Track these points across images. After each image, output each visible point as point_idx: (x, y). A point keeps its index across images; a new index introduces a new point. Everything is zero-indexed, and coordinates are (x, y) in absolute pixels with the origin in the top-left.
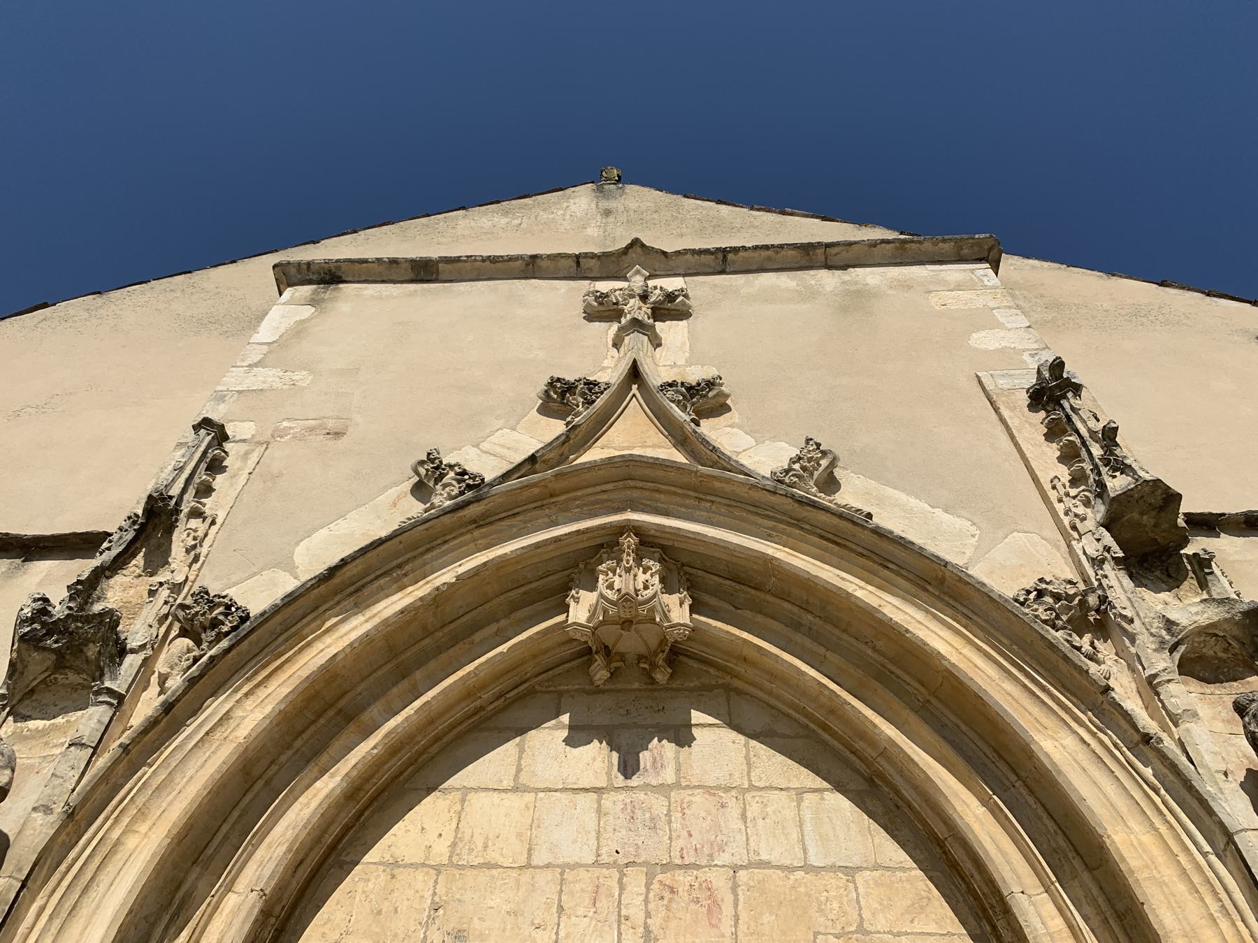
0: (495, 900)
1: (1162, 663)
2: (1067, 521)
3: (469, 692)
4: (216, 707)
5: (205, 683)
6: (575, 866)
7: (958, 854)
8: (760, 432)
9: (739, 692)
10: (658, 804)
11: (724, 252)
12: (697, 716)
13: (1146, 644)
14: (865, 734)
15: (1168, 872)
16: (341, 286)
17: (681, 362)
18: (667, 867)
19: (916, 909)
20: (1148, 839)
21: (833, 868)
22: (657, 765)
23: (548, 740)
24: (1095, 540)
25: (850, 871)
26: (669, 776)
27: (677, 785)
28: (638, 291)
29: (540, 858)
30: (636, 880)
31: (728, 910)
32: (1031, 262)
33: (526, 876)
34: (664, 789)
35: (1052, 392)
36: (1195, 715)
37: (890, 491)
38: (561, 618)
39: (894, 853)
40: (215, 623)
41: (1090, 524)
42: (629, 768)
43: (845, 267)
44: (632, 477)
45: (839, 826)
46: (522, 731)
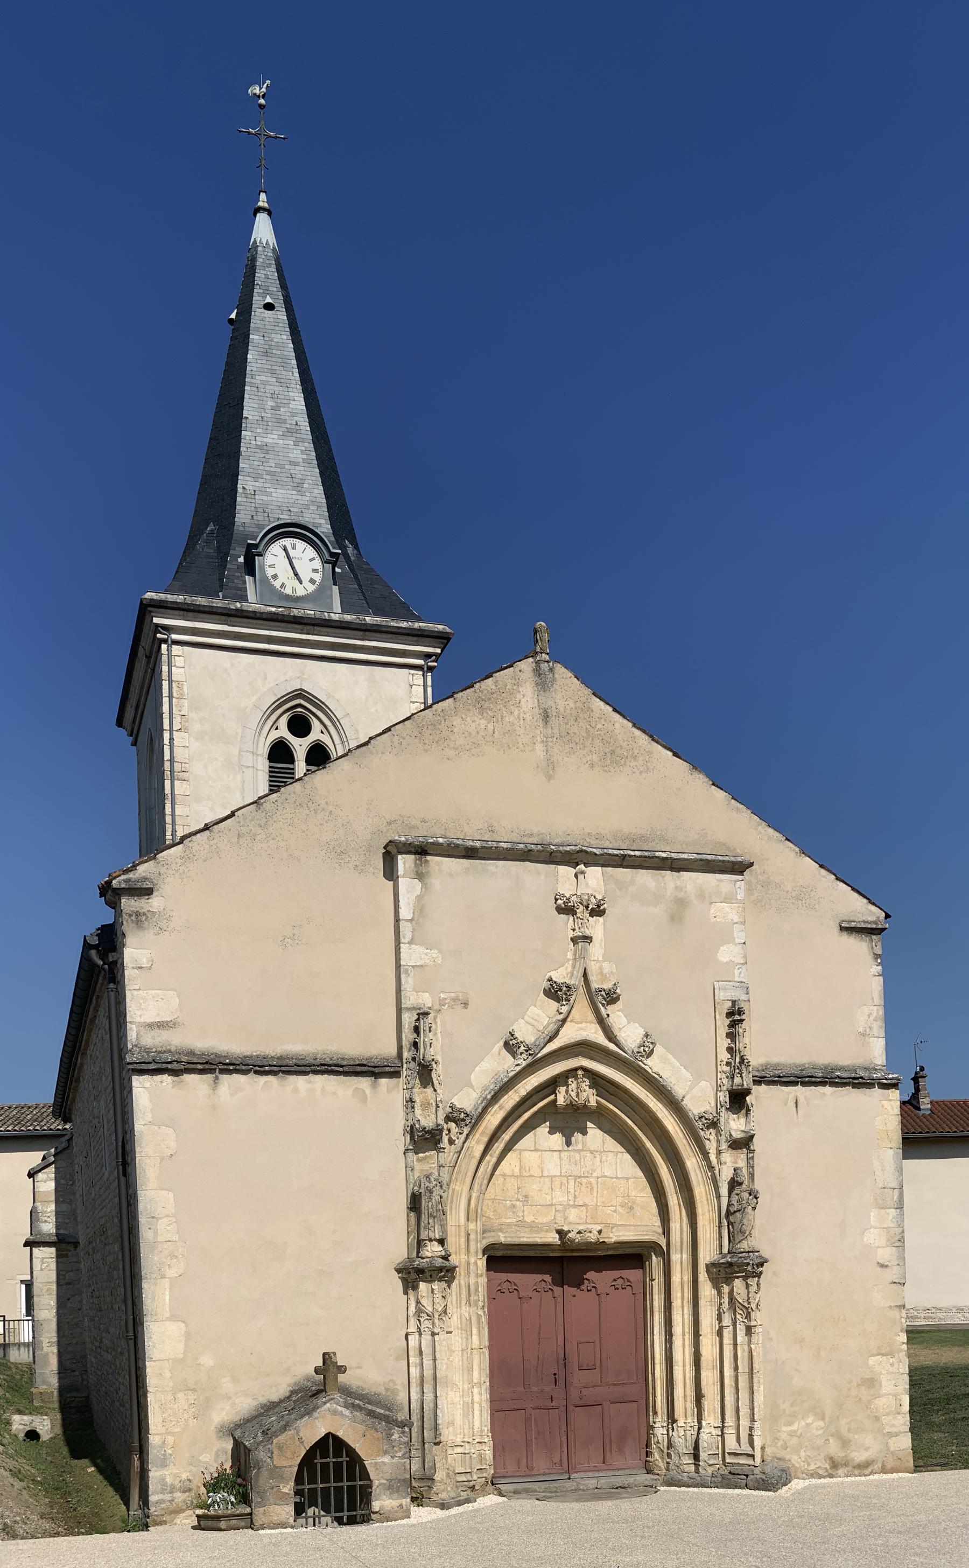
0: (535, 1187)
1: (724, 1146)
2: (719, 1082)
6: (555, 1176)
7: (657, 1179)
9: (603, 1115)
10: (577, 1156)
11: (624, 856)
12: (589, 1124)
13: (723, 1139)
14: (644, 1146)
15: (705, 1198)
16: (429, 858)
17: (600, 959)
18: (580, 1177)
19: (642, 1190)
20: (703, 1190)
21: (623, 1178)
22: (577, 1142)
23: (543, 1130)
24: (724, 1097)
25: (627, 1179)
26: (580, 1146)
27: (582, 1150)
28: (585, 903)
29: (546, 1174)
30: (572, 1182)
31: (595, 1190)
32: (771, 831)
33: (542, 1180)
34: (579, 1151)
35: (735, 1016)
36: (725, 1163)
37: (670, 1056)
38: (553, 1097)
39: (640, 1174)
40: (463, 1120)
41: (724, 1088)
42: (568, 1143)
44: (583, 1047)
45: (626, 1164)
46: (534, 1128)
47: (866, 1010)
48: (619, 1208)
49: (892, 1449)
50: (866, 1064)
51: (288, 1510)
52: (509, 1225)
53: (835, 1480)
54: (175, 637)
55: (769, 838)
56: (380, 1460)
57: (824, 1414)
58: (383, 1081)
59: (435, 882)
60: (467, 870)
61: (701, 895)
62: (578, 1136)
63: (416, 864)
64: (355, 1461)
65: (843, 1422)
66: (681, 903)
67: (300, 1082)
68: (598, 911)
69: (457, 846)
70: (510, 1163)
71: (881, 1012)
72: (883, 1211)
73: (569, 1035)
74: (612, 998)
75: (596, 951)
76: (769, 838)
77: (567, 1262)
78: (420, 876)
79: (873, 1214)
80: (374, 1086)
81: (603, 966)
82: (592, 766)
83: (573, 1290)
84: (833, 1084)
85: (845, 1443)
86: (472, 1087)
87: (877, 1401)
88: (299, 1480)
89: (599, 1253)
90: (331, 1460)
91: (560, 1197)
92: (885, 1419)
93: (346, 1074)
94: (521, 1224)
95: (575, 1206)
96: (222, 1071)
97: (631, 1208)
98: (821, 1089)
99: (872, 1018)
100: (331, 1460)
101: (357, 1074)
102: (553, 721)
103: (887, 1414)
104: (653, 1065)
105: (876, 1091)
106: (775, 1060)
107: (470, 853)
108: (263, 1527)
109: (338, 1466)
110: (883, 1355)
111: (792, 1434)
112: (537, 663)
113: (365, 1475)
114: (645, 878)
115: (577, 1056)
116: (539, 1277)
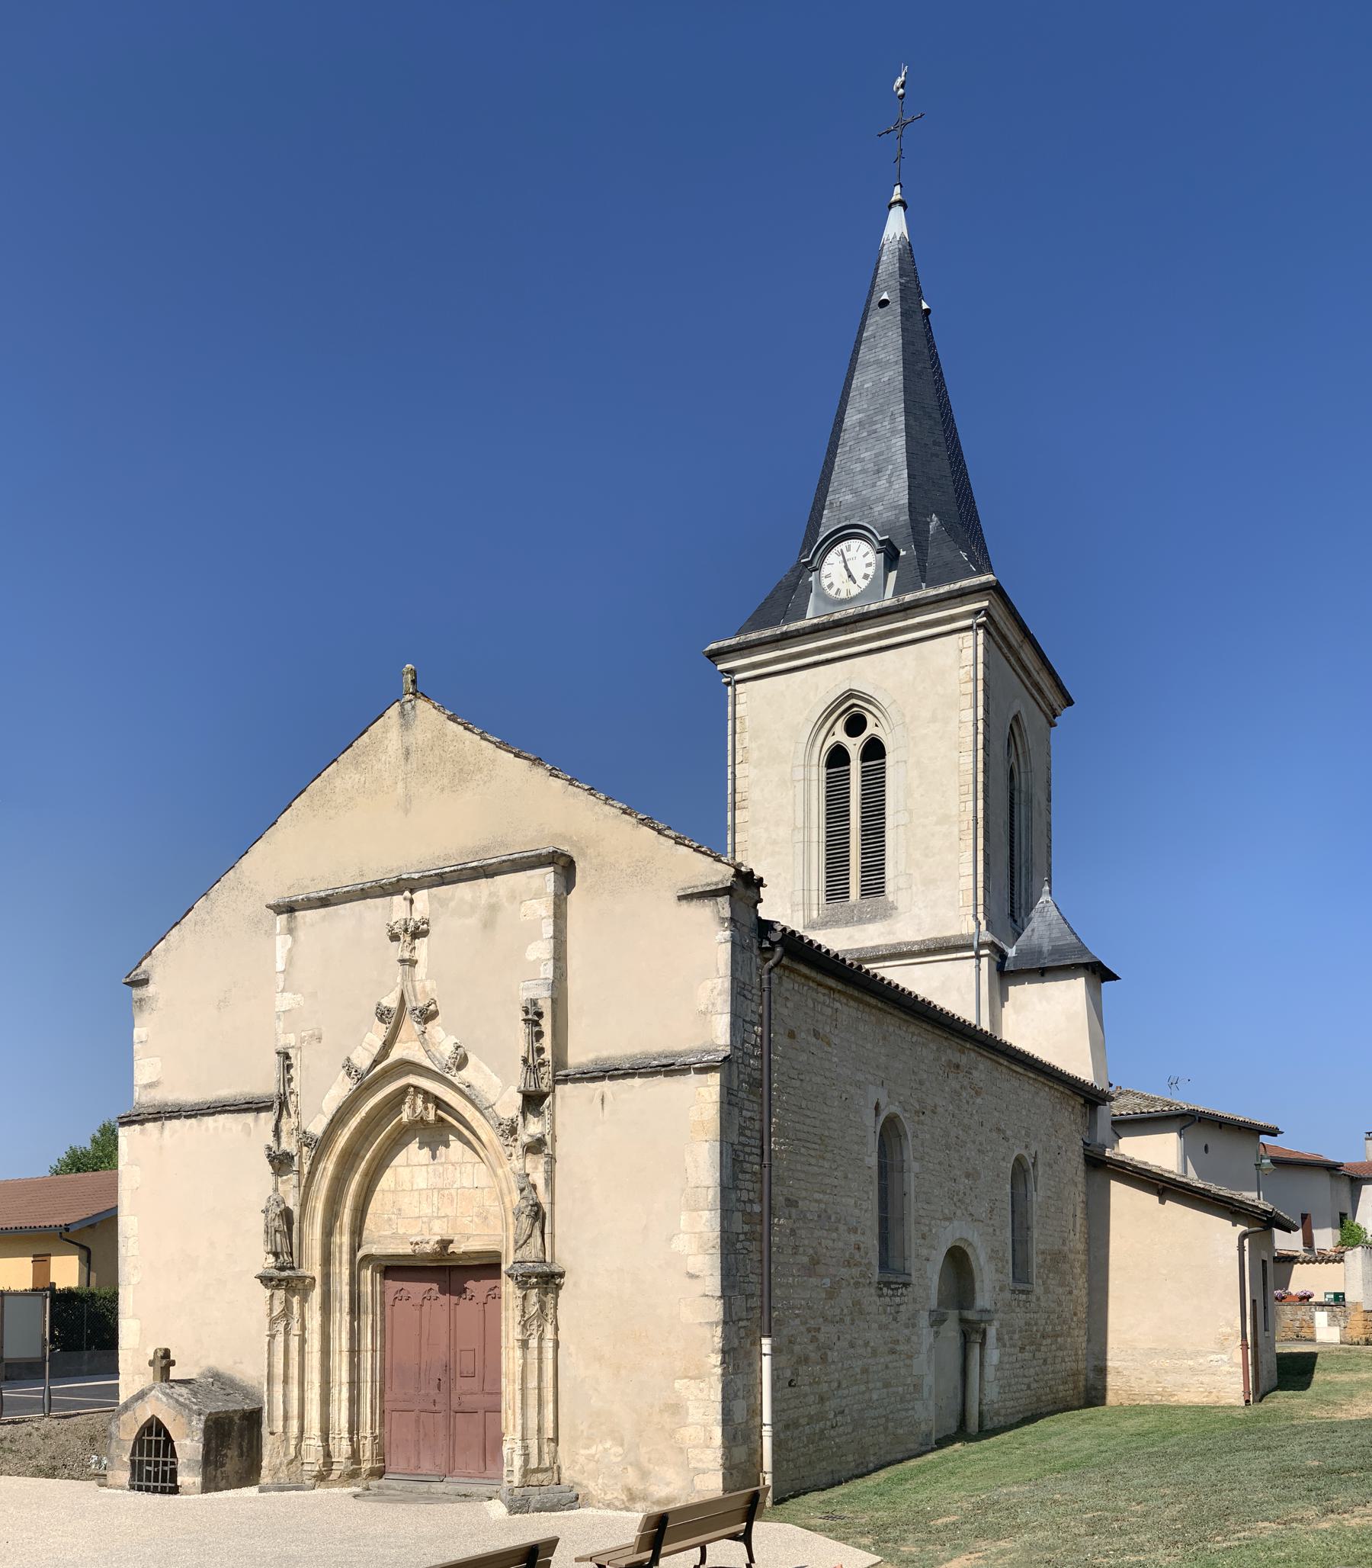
3: (388, 1137)
4: (321, 1166)
5: (315, 1162)
8: (448, 1032)
12: (451, 1137)
23: (414, 1145)
24: (519, 1099)
37: (482, 1064)
43: (492, 876)
47: (709, 984)
48: (476, 1219)
49: (698, 1487)
50: (708, 1046)
51: (124, 1476)
52: (385, 1237)
53: (629, 1514)
54: (738, 677)
55: (606, 816)
56: (183, 1442)
57: (622, 1440)
58: (263, 1115)
59: (301, 934)
60: (324, 918)
61: (513, 896)
62: (442, 1149)
63: (289, 922)
64: (169, 1440)
65: (643, 1450)
66: (493, 908)
67: (209, 1120)
68: (417, 934)
69: (309, 899)
70: (386, 1181)
71: (727, 984)
72: (695, 1214)
73: (396, 1054)
74: (427, 1016)
75: (420, 971)
76: (606, 816)
77: (451, 1272)
78: (290, 931)
79: (684, 1217)
80: (256, 1120)
81: (425, 985)
82: (443, 790)
83: (454, 1299)
84: (641, 1075)
85: (644, 1474)
86: (323, 1113)
87: (682, 1430)
88: (133, 1454)
89: (460, 1263)
90: (153, 1438)
91: (426, 1209)
92: (692, 1453)
93: (239, 1111)
94: (394, 1236)
95: (438, 1218)
96: (167, 1118)
97: (486, 1218)
98: (629, 1081)
99: (716, 992)
100: (153, 1438)
101: (245, 1111)
102: (413, 758)
103: (694, 1447)
104: (458, 1078)
105: (693, 1078)
106: (605, 1054)
107: (324, 902)
108: (110, 1487)
109: (158, 1442)
110: (691, 1378)
111: (590, 1458)
112: (402, 705)
113: (174, 1455)
114: (463, 891)
115: (407, 1074)
116: (428, 1286)
